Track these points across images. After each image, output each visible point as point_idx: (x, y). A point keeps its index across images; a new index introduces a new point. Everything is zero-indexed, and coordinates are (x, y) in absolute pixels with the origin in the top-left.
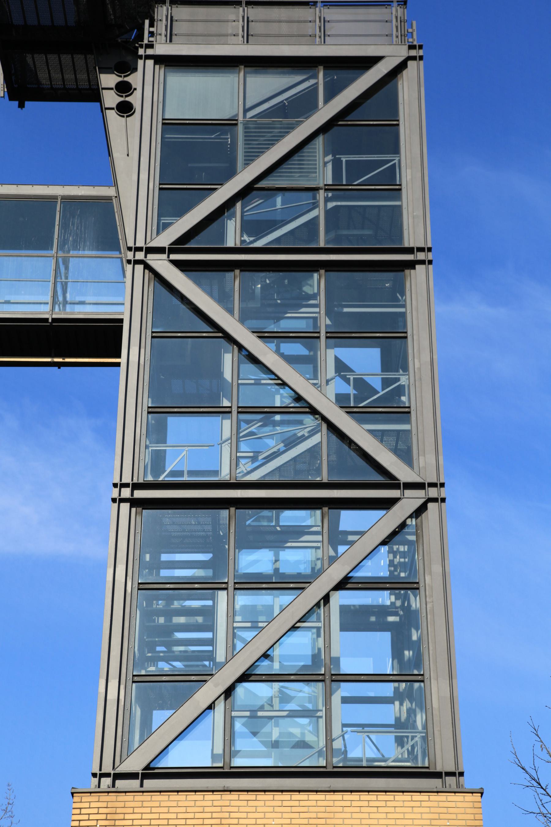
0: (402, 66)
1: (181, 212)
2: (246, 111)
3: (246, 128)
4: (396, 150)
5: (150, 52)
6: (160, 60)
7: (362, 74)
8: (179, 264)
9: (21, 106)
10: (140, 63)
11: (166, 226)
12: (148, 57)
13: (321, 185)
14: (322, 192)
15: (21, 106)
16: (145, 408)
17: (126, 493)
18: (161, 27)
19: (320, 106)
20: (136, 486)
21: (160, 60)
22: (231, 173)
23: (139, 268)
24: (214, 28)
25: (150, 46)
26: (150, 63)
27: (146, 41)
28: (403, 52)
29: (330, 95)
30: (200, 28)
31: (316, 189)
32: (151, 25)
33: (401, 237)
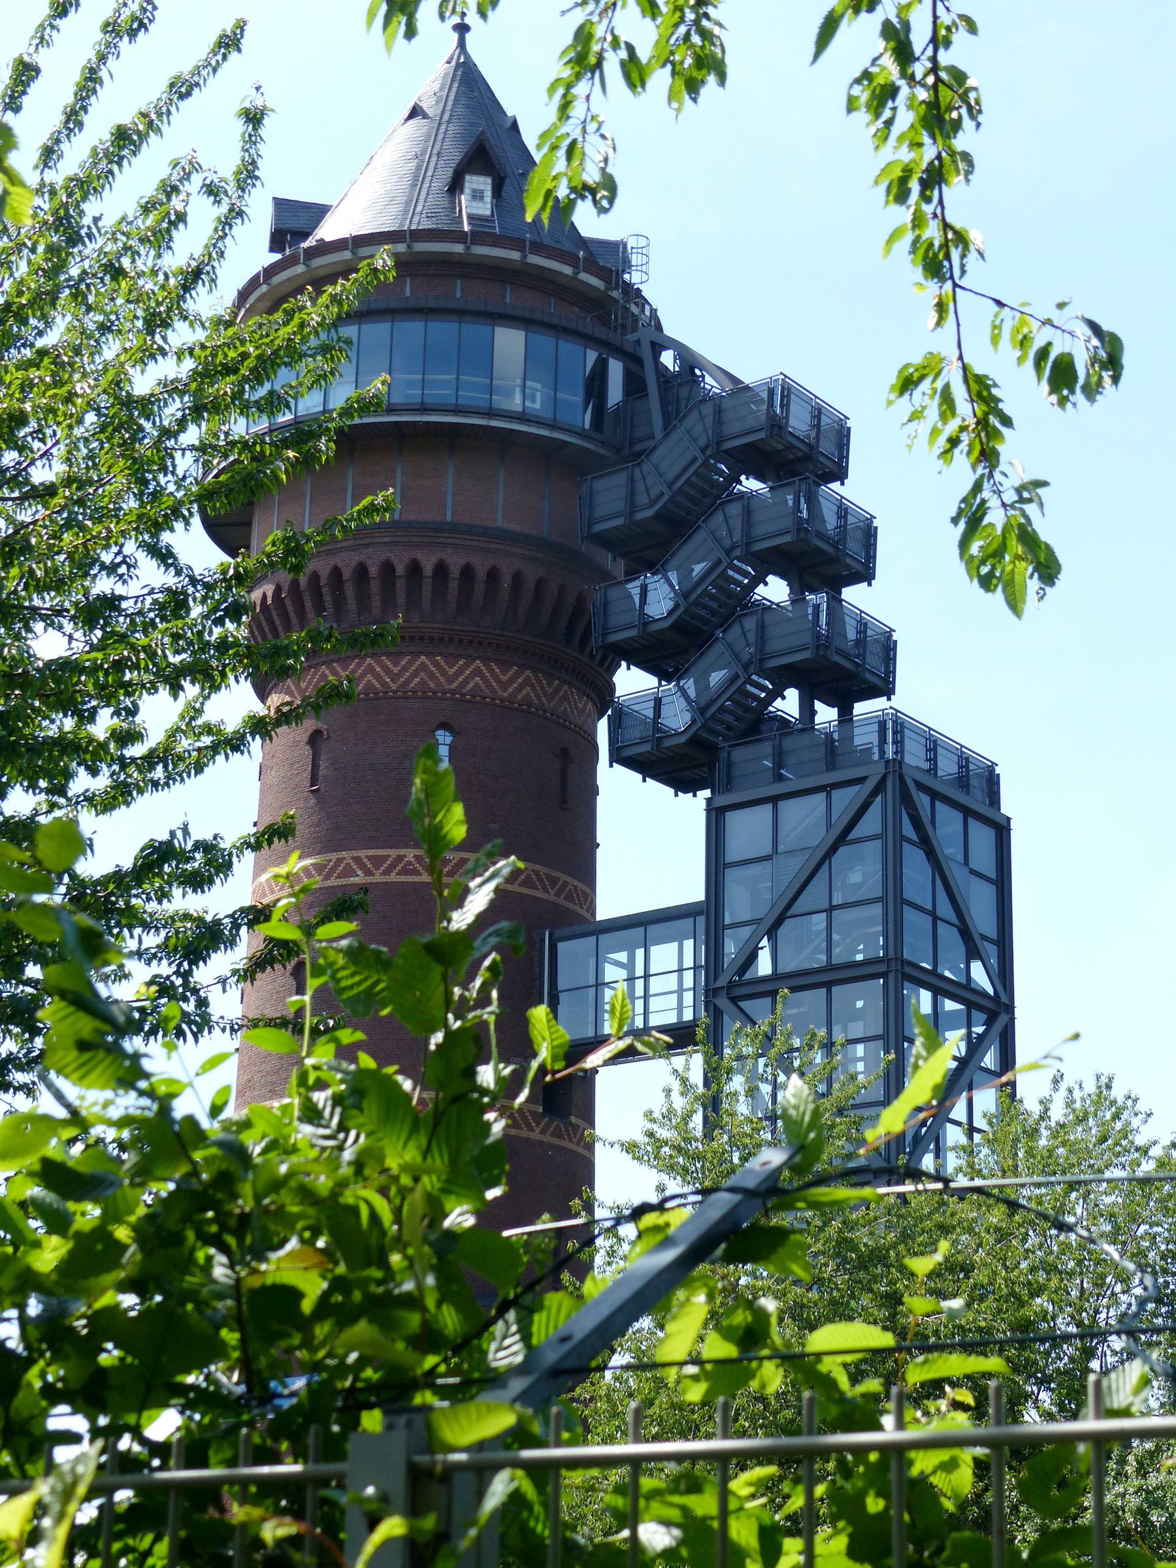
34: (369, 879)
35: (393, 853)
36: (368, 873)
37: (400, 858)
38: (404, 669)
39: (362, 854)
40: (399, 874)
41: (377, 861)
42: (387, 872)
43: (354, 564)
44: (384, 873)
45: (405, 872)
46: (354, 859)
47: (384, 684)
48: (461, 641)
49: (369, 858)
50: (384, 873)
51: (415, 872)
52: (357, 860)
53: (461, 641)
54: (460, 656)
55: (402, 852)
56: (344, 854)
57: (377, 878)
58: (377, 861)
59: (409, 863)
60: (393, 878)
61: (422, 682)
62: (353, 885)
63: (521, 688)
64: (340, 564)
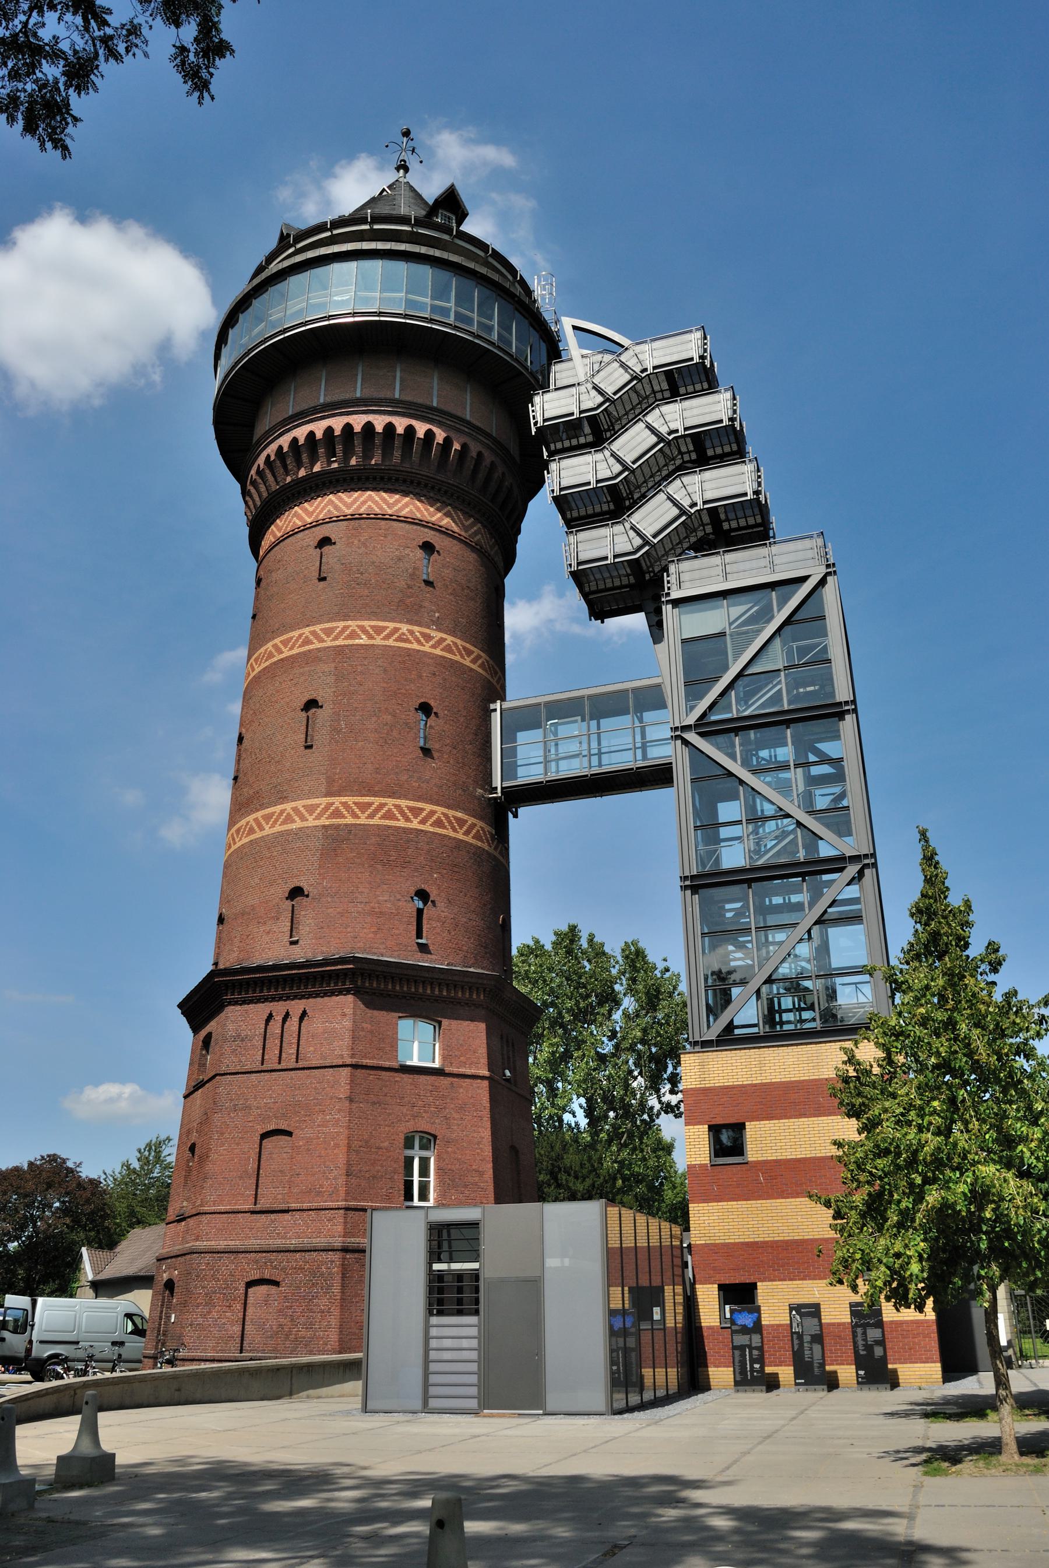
0: (822, 582)
1: (701, 697)
2: (730, 624)
3: (731, 635)
4: (824, 633)
5: (668, 599)
6: (676, 603)
7: (802, 586)
8: (702, 735)
9: (603, 622)
10: (664, 607)
11: (692, 708)
12: (668, 602)
13: (781, 667)
14: (782, 673)
15: (603, 622)
16: (692, 827)
17: (688, 883)
18: (673, 578)
19: (776, 614)
20: (693, 877)
21: (676, 603)
22: (726, 668)
23: (679, 742)
24: (705, 573)
25: (668, 594)
26: (670, 606)
27: (666, 591)
28: (823, 570)
29: (782, 604)
30: (697, 575)
31: (779, 670)
32: (668, 576)
33: (833, 694)
34: (371, 642)
35: (391, 625)
36: (371, 637)
37: (396, 630)
38: (397, 502)
39: (366, 623)
40: (396, 640)
41: (379, 630)
42: (387, 637)
43: (363, 423)
44: (384, 639)
45: (399, 639)
46: (358, 626)
47: (381, 508)
48: (439, 490)
49: (372, 627)
50: (384, 639)
51: (407, 641)
52: (363, 629)
53: (439, 490)
54: (438, 500)
55: (398, 625)
56: (350, 623)
57: (378, 641)
58: (379, 630)
59: (403, 634)
60: (391, 642)
61: (411, 511)
62: (357, 645)
63: (476, 533)
64: (351, 422)
